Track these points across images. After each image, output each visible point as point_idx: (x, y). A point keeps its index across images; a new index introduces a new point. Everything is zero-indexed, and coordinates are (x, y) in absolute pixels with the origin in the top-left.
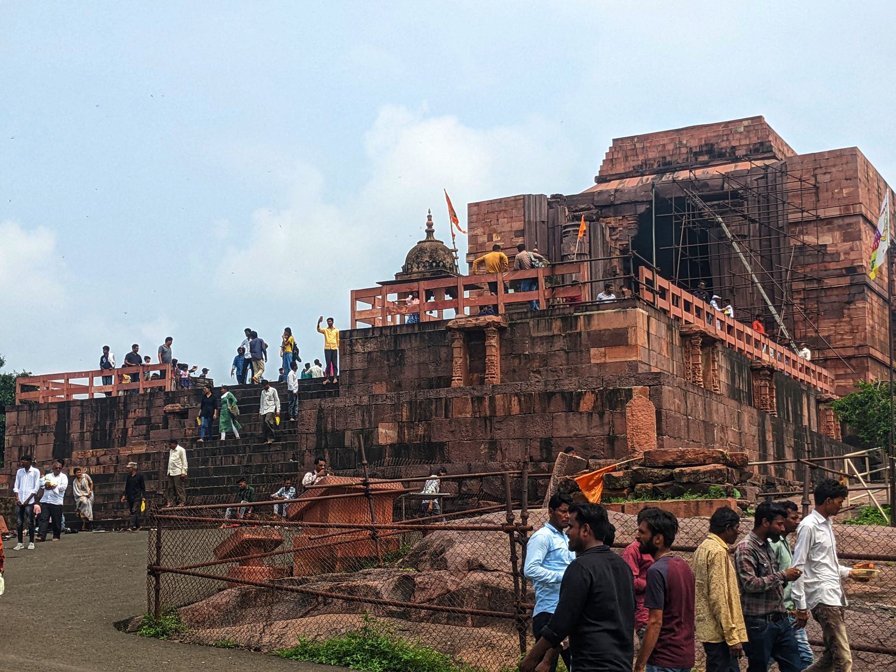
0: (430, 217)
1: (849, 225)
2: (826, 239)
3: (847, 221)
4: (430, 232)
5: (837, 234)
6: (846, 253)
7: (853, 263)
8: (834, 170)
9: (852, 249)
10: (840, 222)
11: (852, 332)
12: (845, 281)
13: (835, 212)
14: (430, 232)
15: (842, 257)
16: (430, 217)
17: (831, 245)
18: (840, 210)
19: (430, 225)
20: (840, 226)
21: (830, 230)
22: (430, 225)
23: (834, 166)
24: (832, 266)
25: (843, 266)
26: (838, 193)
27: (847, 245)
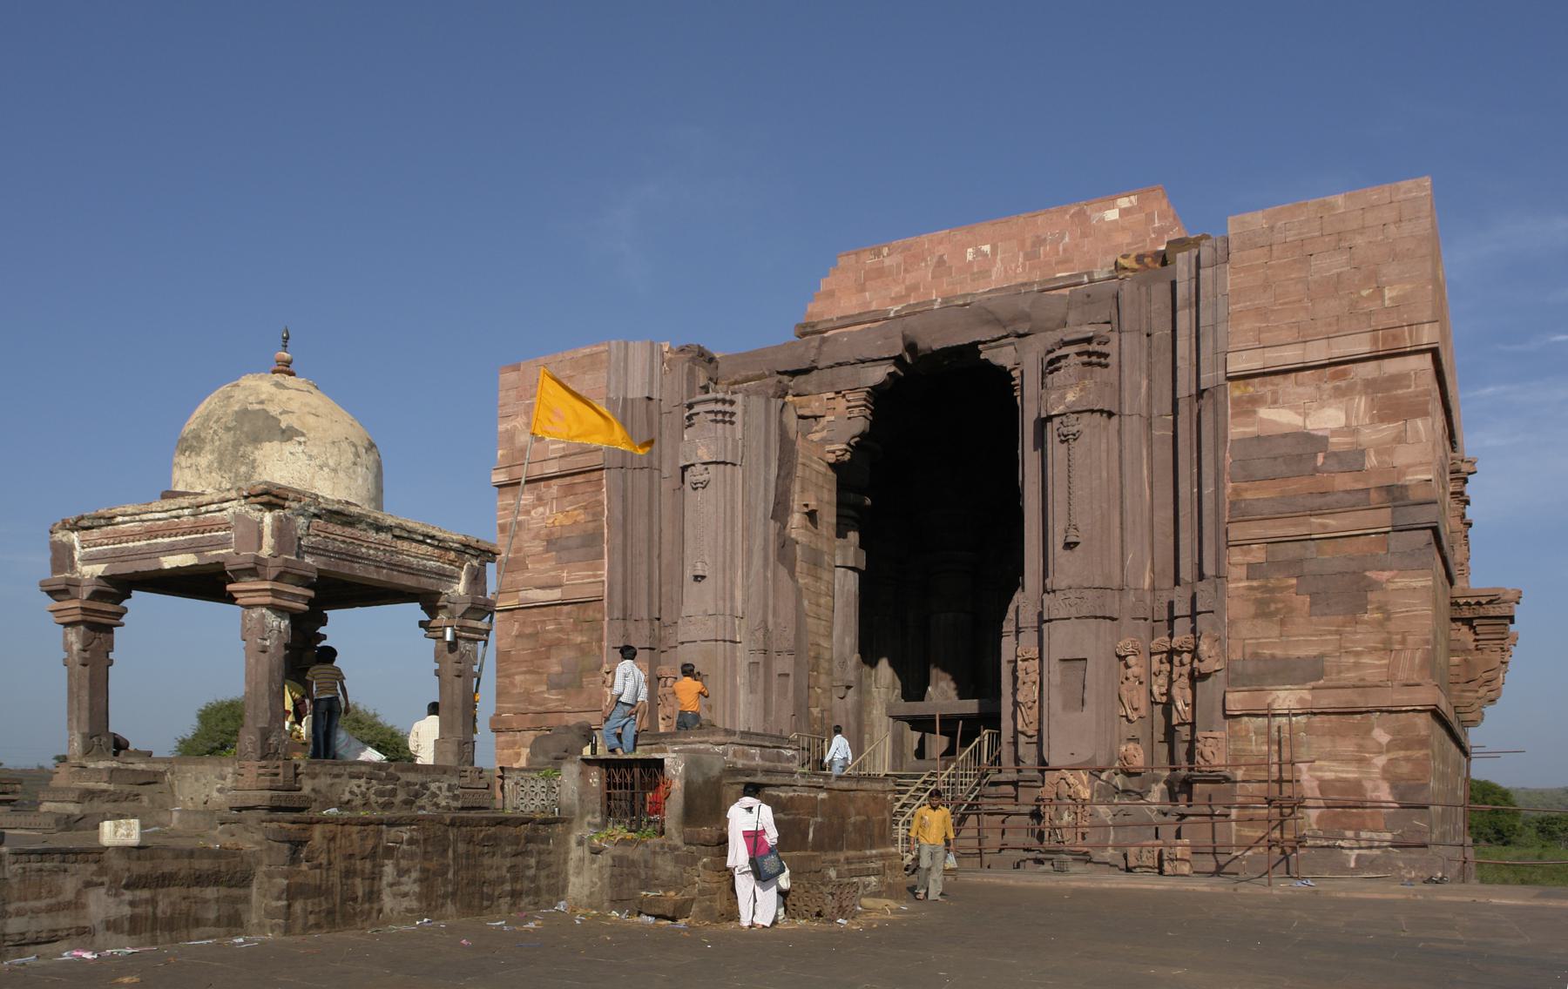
1: (1396, 380)
2: (1328, 419)
3: (1393, 366)
5: (1361, 403)
8: (1360, 241)
18: (1375, 341)
20: (1370, 386)
21: (1339, 393)
23: (1362, 230)
24: (1343, 482)
26: (1369, 298)
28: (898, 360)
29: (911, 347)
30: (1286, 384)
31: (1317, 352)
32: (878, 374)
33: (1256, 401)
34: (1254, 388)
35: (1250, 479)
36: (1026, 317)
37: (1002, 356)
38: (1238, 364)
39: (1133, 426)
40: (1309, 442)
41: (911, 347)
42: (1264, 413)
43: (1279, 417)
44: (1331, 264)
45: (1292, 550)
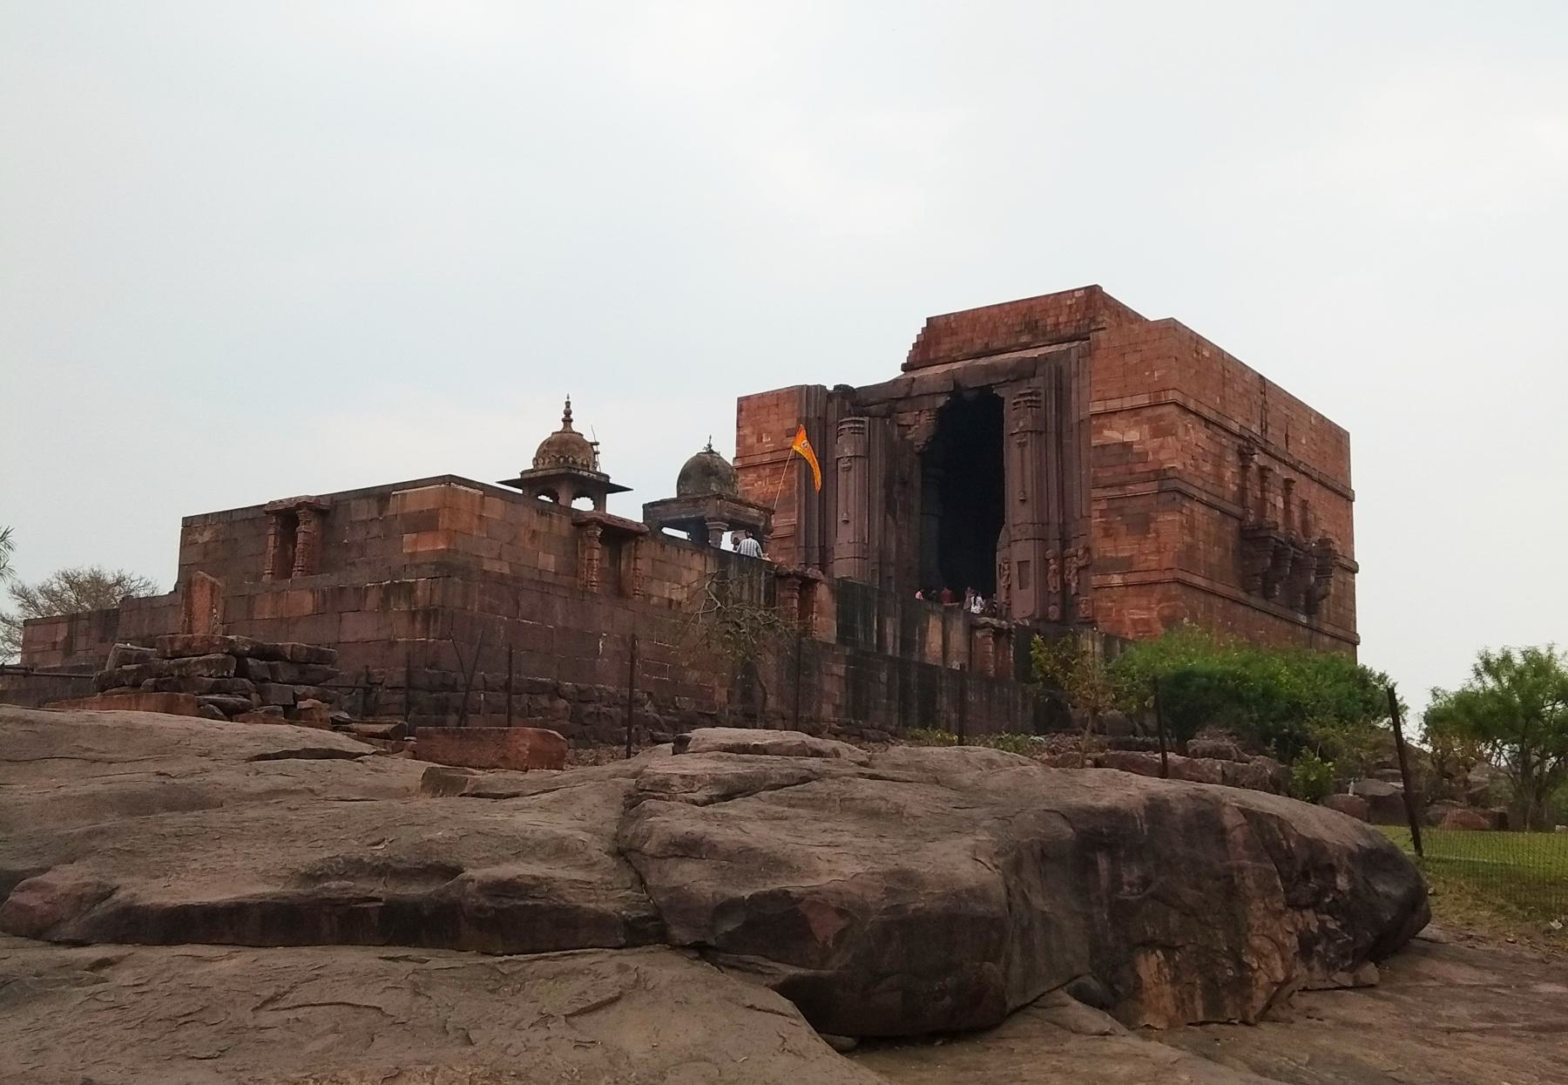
0: (568, 404)
1: (1161, 417)
2: (1133, 436)
4: (567, 420)
6: (1156, 452)
7: (1162, 464)
8: (1144, 347)
9: (1162, 447)
10: (1148, 413)
11: (1158, 551)
12: (1153, 487)
13: (1143, 400)
14: (567, 420)
15: (1151, 457)
16: (568, 404)
17: (1138, 443)
19: (568, 413)
20: (1149, 419)
22: (568, 413)
23: (1145, 342)
24: (1139, 468)
25: (1150, 467)
27: (1157, 442)
28: (950, 393)
29: (956, 385)
30: (1116, 419)
31: (1128, 403)
32: (941, 401)
33: (1103, 427)
34: (1102, 421)
35: (1102, 467)
36: (1012, 371)
37: (1001, 392)
38: (1098, 407)
39: (1053, 437)
40: (1127, 446)
41: (956, 385)
42: (1106, 433)
43: (1112, 435)
44: (1132, 359)
45: (1117, 504)
